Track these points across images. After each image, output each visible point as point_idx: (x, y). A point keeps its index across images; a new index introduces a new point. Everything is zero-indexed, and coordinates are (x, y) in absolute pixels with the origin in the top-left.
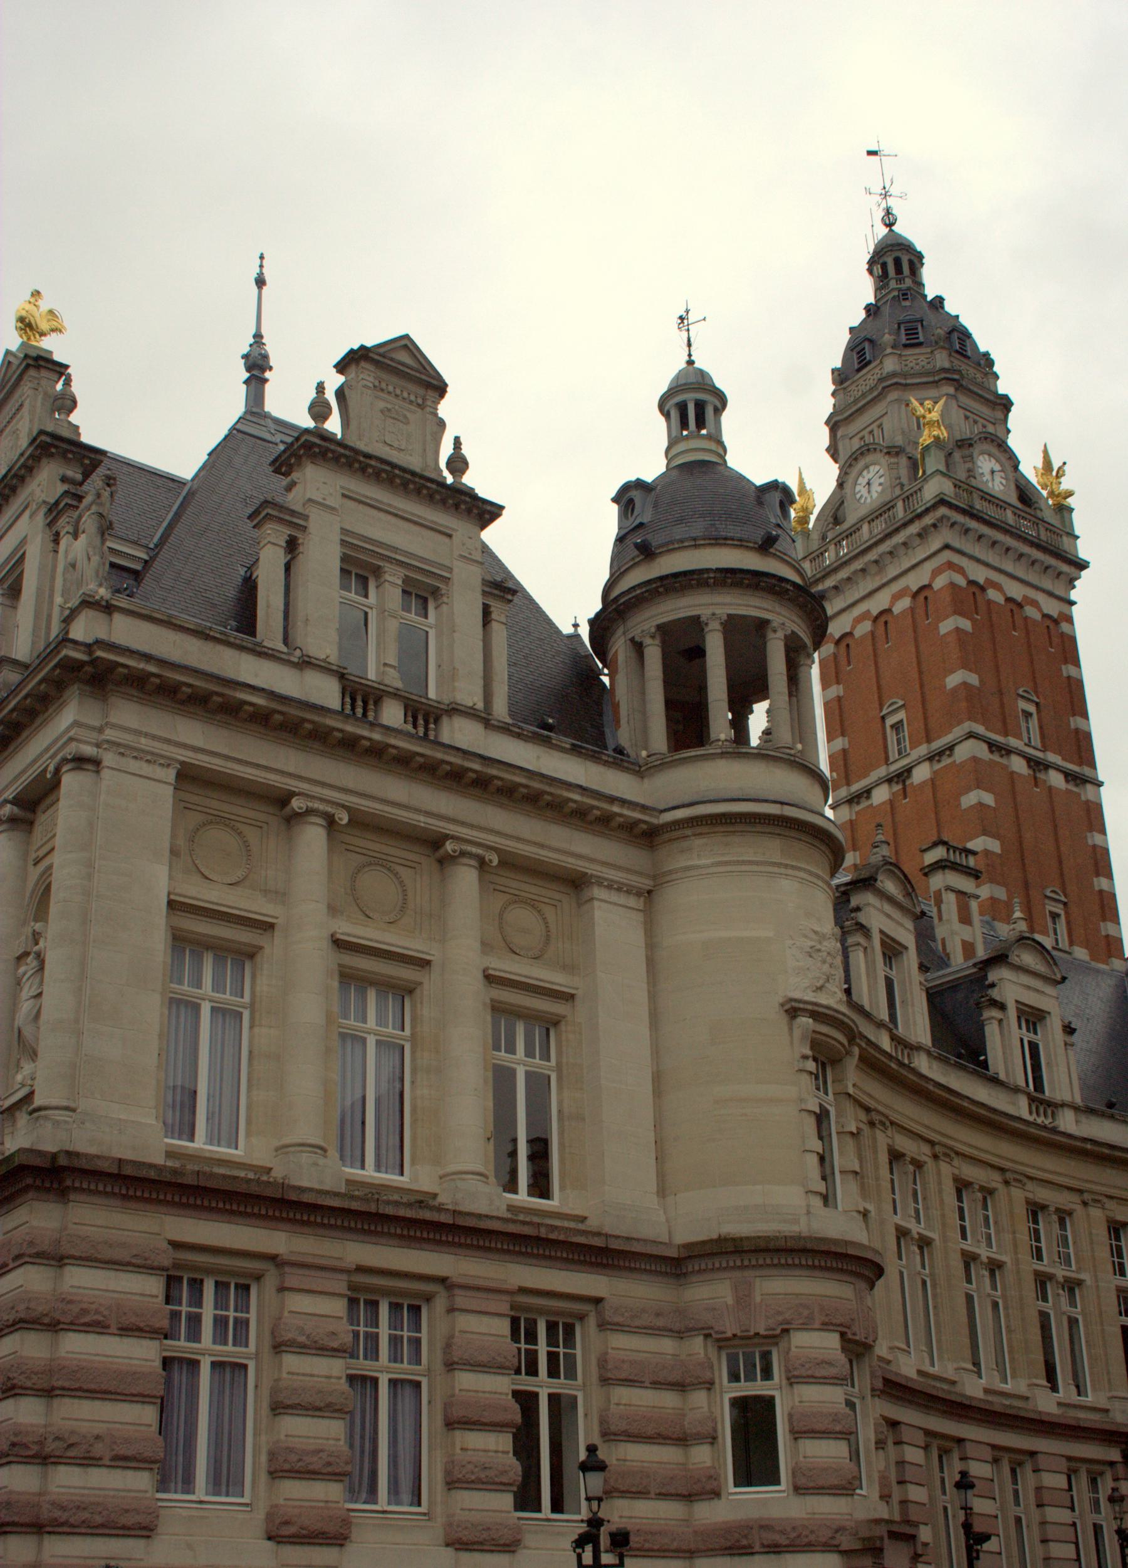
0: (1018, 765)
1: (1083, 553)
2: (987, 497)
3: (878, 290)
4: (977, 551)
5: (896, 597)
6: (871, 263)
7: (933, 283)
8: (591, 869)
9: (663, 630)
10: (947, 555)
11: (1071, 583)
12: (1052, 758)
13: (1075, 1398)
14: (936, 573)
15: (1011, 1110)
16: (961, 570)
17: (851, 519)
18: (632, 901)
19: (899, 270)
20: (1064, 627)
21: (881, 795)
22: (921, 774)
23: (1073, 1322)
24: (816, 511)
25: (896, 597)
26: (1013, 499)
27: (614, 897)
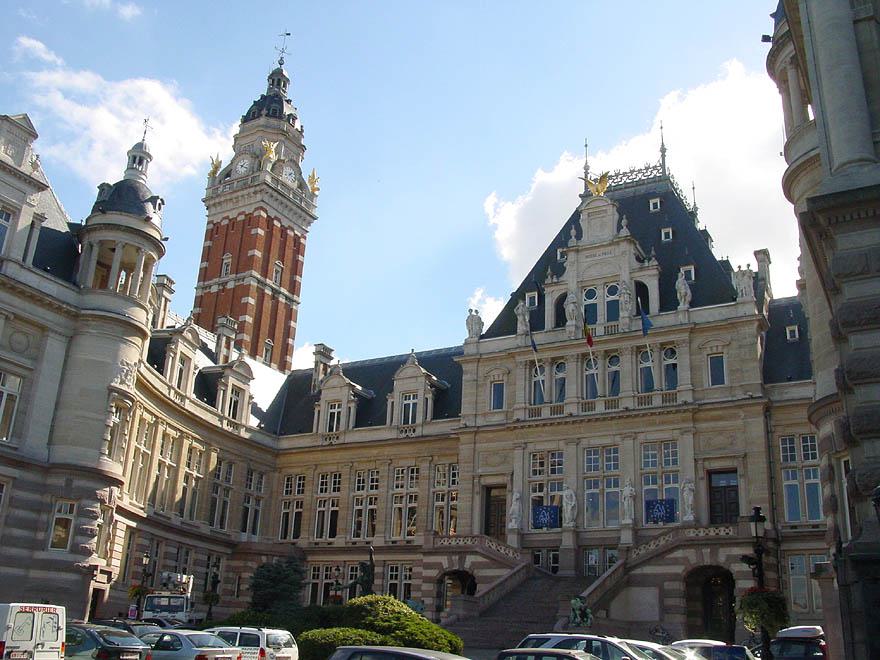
0: (268, 292)
1: (315, 212)
2: (284, 185)
3: (269, 89)
4: (275, 205)
5: (240, 214)
6: (269, 78)
7: (290, 92)
8: (49, 324)
9: (102, 243)
10: (262, 204)
11: (309, 224)
12: (283, 290)
13: (219, 530)
14: (256, 209)
15: (219, 424)
16: (266, 211)
17: (233, 177)
18: (64, 339)
19: (279, 84)
20: (302, 240)
21: (214, 289)
22: (231, 285)
23: (225, 503)
24: (221, 170)
25: (240, 214)
26: (295, 185)
27: (57, 337)
